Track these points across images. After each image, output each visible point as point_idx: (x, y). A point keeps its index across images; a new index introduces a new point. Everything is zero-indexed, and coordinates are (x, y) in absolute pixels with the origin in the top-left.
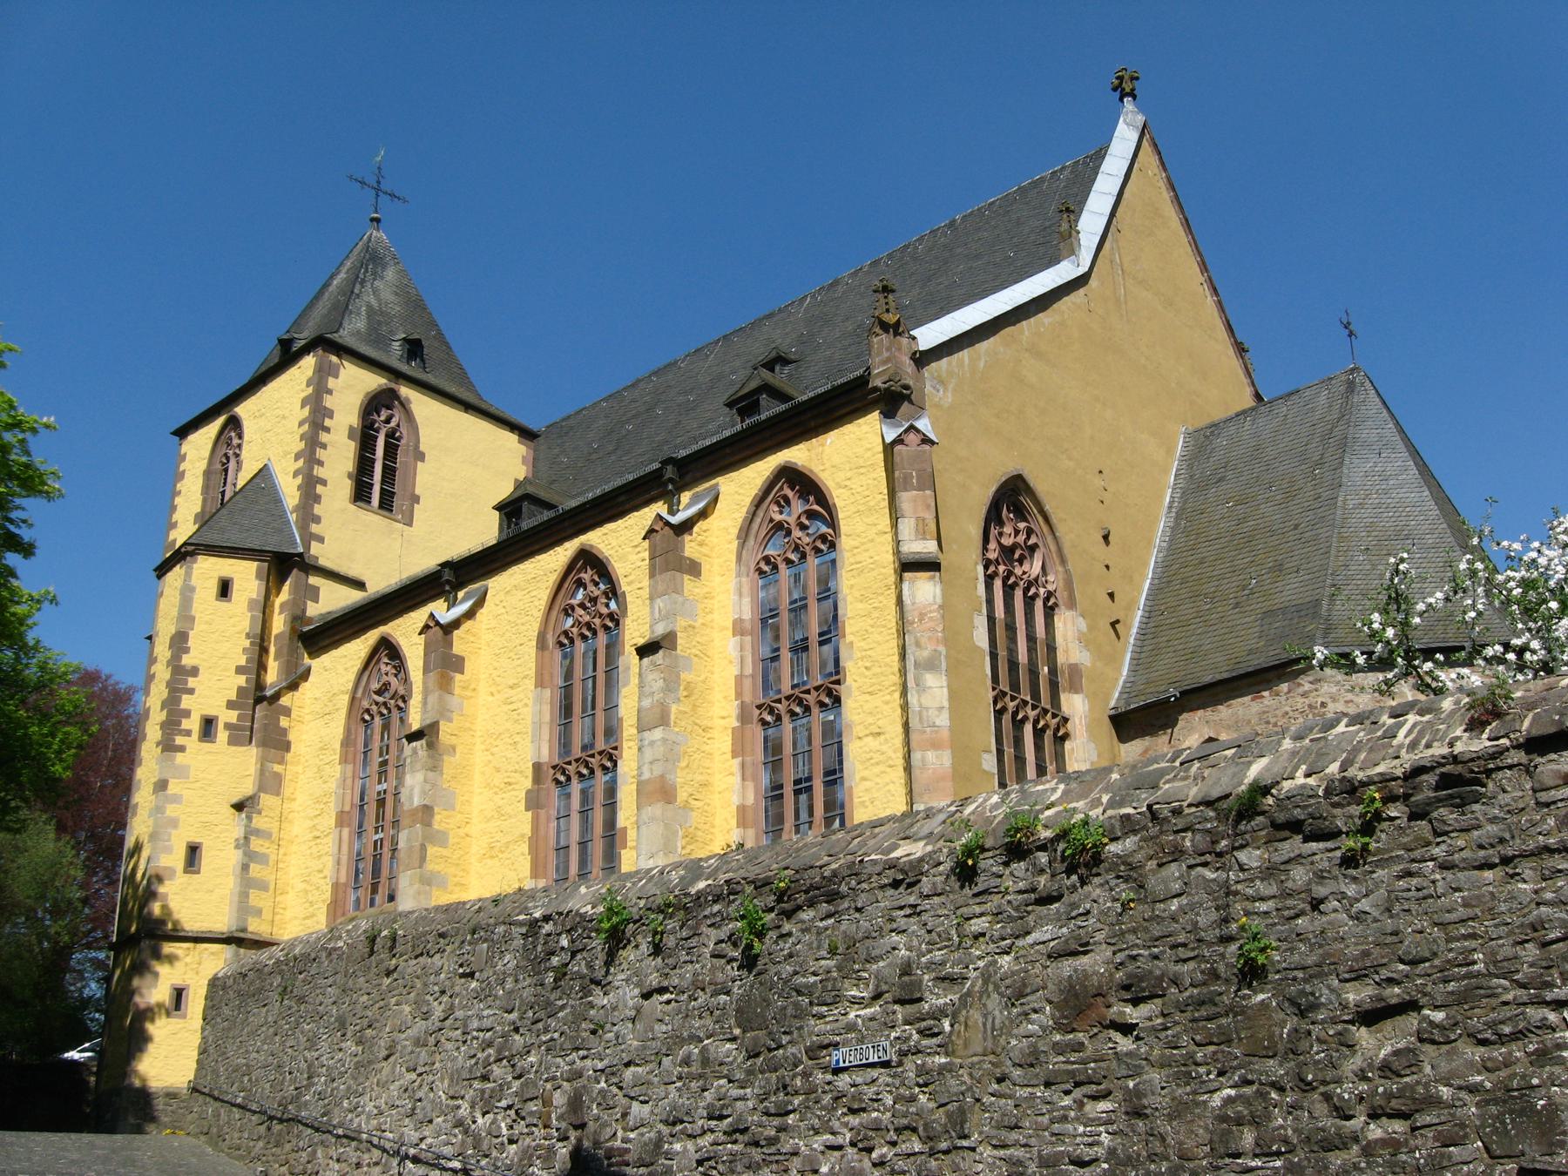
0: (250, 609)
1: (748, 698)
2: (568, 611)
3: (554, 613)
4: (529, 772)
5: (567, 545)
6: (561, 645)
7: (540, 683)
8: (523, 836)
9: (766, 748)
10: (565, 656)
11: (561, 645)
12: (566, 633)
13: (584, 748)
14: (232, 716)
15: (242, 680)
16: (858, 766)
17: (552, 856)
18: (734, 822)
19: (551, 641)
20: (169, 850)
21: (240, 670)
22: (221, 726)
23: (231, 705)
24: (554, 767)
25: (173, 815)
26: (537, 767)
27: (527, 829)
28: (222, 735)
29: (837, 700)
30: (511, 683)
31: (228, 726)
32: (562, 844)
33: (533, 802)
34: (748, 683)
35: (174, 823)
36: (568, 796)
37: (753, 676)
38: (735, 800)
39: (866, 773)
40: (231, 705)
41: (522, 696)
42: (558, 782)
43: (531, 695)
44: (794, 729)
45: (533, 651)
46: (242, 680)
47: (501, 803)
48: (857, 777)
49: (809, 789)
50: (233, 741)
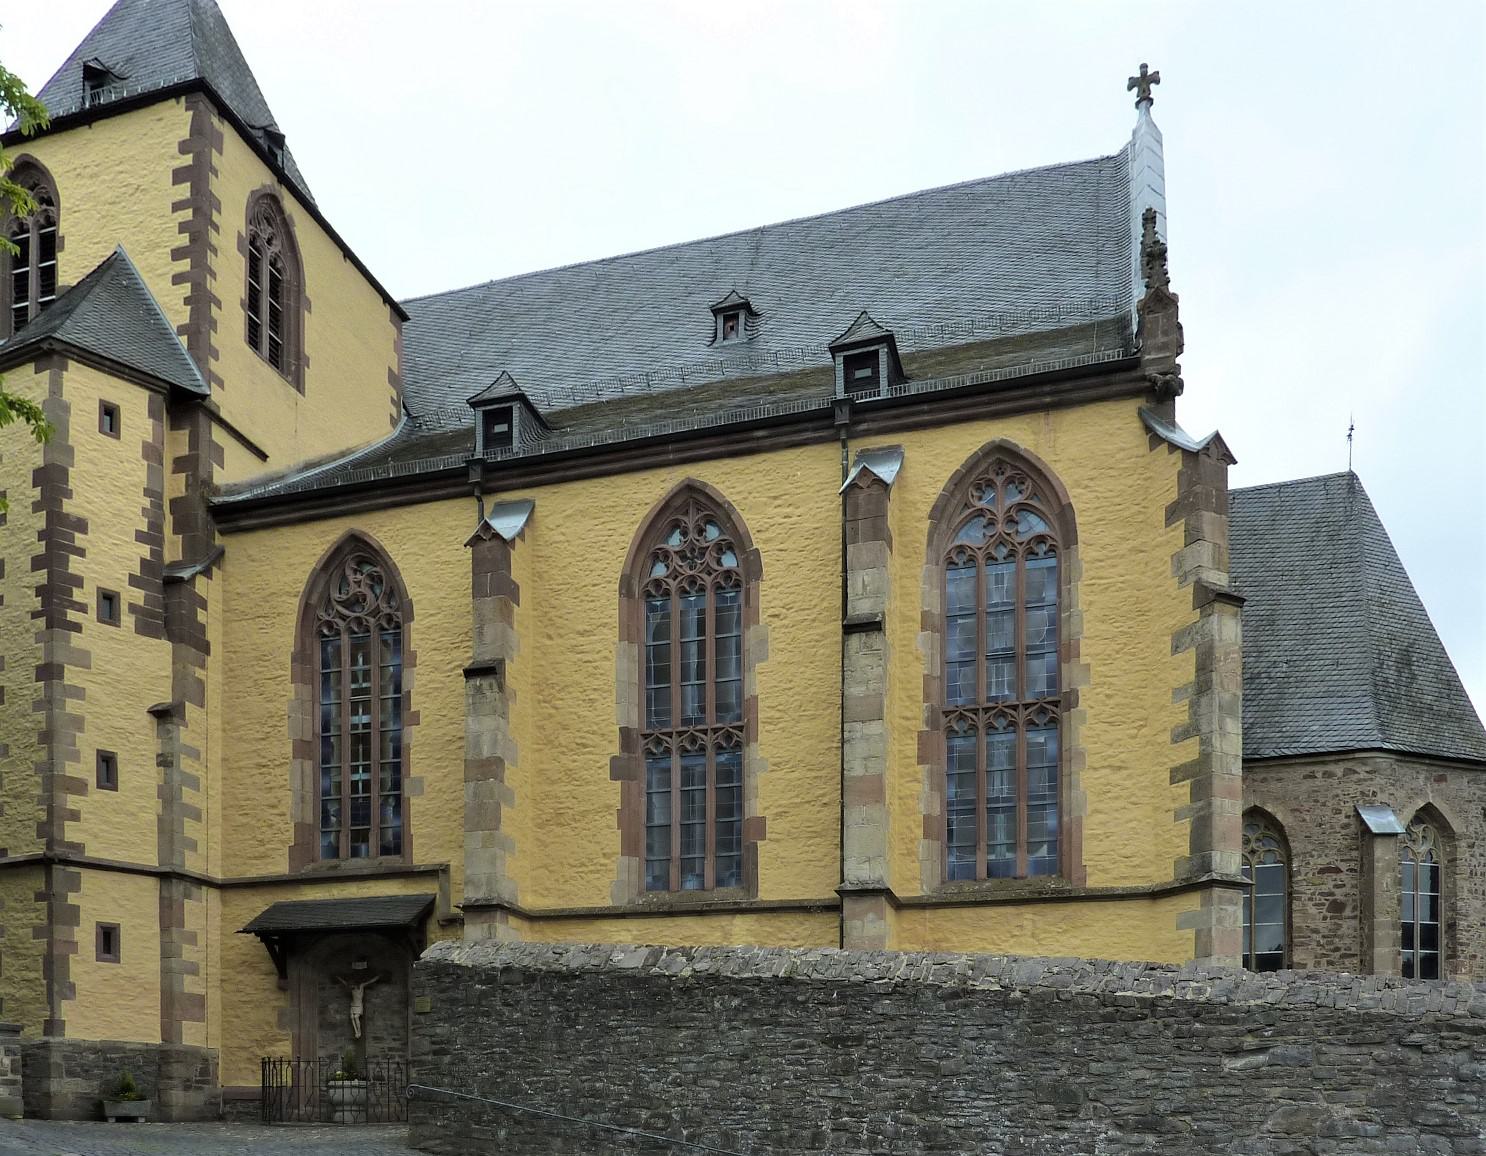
0: (146, 456)
1: (935, 702)
2: (662, 556)
3: (642, 556)
4: (616, 738)
5: (663, 473)
6: (649, 595)
7: (627, 634)
8: (609, 807)
9: (950, 760)
10: (652, 609)
11: (649, 595)
12: (657, 583)
13: (686, 721)
14: (138, 596)
15: (145, 551)
16: (1091, 797)
17: (644, 832)
18: (920, 832)
19: (637, 590)
20: (75, 756)
21: (141, 537)
22: (124, 607)
23: (134, 581)
24: (645, 736)
25: (78, 712)
26: (625, 733)
27: (616, 801)
28: (128, 620)
29: (1054, 722)
30: (580, 628)
31: (133, 608)
32: (658, 820)
33: (618, 770)
34: (935, 685)
35: (78, 723)
36: (668, 770)
37: (941, 678)
38: (922, 808)
39: (1101, 806)
40: (134, 581)
41: (599, 647)
42: (649, 753)
43: (612, 648)
44: (990, 745)
45: (615, 598)
46: (145, 551)
47: (572, 765)
48: (1089, 808)
49: (1011, 811)
50: (145, 628)
